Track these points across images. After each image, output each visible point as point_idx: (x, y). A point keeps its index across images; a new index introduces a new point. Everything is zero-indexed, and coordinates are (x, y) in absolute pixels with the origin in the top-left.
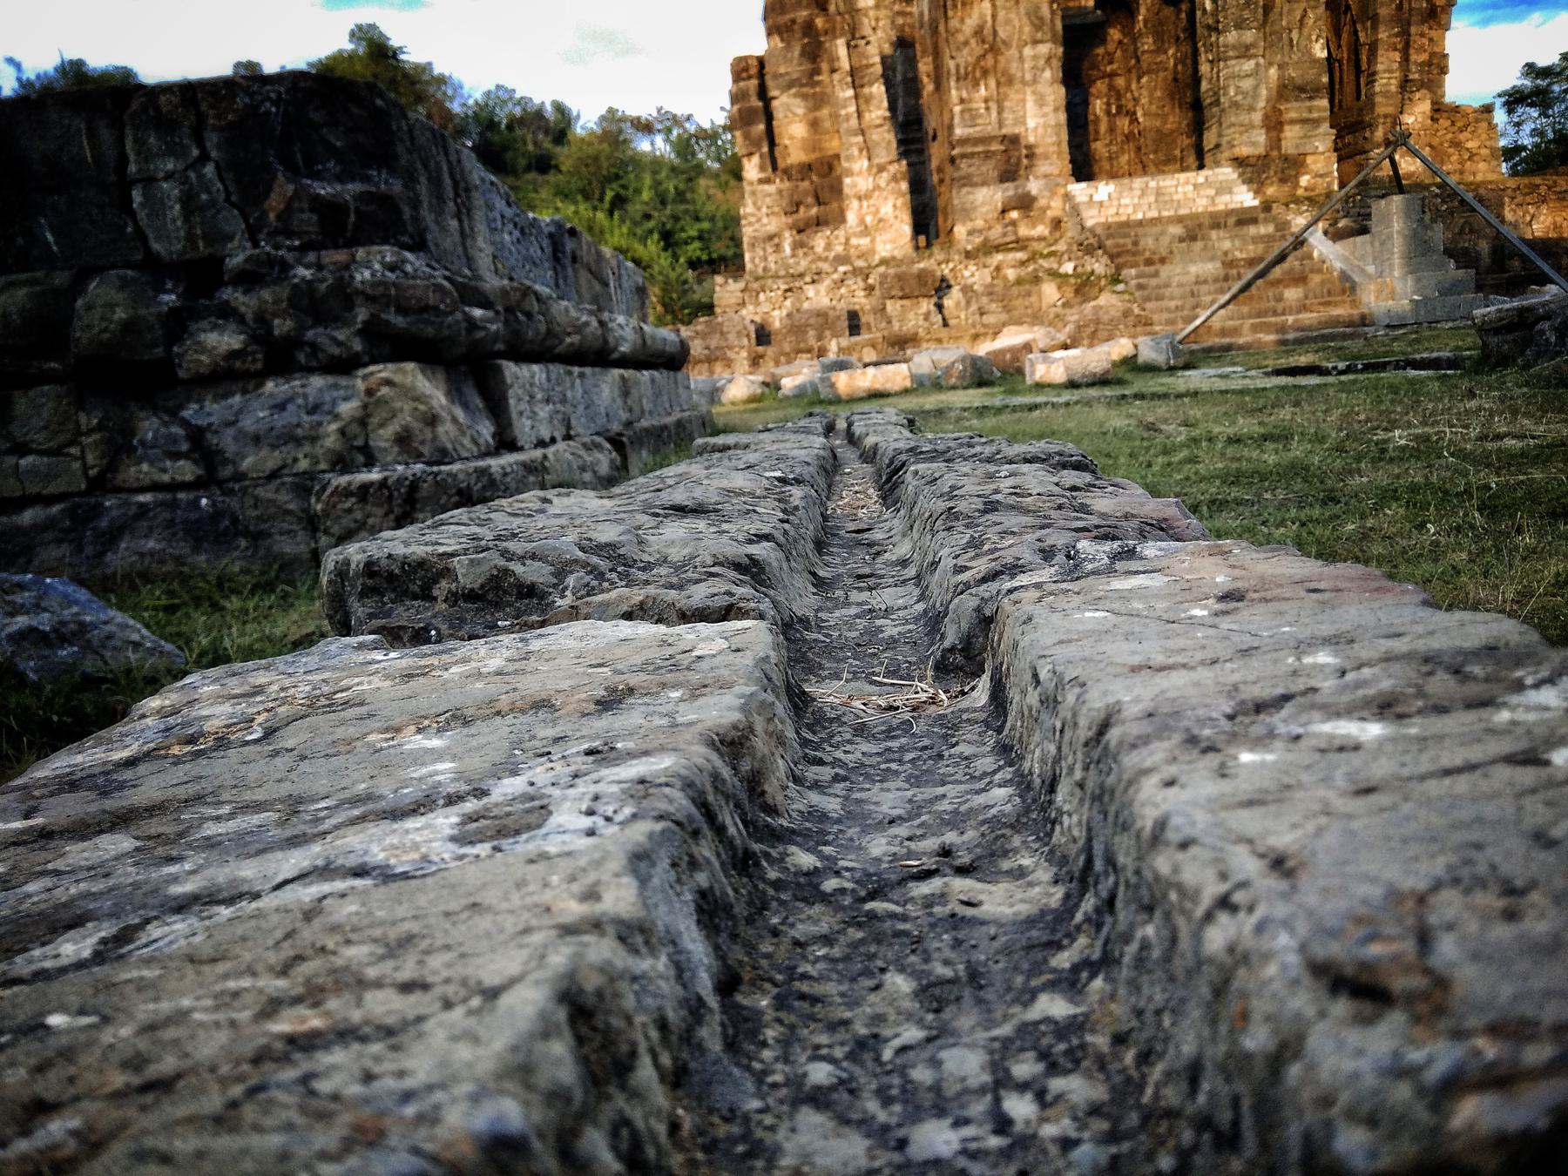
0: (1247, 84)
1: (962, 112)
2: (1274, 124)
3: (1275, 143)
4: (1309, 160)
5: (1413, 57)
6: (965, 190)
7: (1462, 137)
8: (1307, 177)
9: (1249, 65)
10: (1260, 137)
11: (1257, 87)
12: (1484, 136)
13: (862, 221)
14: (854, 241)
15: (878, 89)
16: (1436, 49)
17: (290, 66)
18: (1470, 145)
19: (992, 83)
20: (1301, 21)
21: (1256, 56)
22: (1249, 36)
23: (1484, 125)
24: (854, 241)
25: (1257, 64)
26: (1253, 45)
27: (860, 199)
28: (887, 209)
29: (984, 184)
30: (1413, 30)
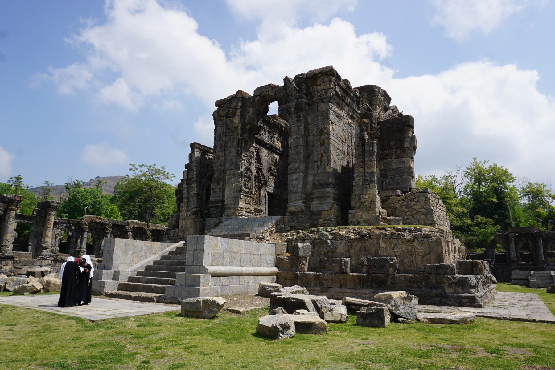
0: (295, 183)
1: (213, 192)
2: (308, 199)
3: (308, 206)
4: (323, 213)
5: (367, 170)
6: (209, 219)
7: (412, 203)
8: (321, 220)
9: (295, 176)
10: (300, 204)
11: (298, 184)
12: (423, 204)
13: (182, 227)
14: (179, 234)
15: (194, 185)
16: (406, 165)
17: (109, 176)
18: (416, 207)
19: (222, 183)
20: (321, 158)
21: (299, 172)
22: (297, 165)
23: (423, 199)
24: (179, 234)
25: (299, 176)
26: (298, 168)
27: (183, 220)
28: (188, 223)
29: (215, 217)
30: (366, 159)
